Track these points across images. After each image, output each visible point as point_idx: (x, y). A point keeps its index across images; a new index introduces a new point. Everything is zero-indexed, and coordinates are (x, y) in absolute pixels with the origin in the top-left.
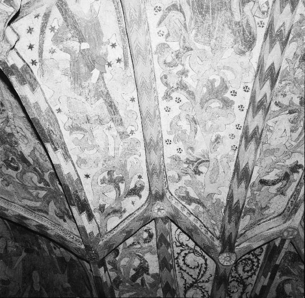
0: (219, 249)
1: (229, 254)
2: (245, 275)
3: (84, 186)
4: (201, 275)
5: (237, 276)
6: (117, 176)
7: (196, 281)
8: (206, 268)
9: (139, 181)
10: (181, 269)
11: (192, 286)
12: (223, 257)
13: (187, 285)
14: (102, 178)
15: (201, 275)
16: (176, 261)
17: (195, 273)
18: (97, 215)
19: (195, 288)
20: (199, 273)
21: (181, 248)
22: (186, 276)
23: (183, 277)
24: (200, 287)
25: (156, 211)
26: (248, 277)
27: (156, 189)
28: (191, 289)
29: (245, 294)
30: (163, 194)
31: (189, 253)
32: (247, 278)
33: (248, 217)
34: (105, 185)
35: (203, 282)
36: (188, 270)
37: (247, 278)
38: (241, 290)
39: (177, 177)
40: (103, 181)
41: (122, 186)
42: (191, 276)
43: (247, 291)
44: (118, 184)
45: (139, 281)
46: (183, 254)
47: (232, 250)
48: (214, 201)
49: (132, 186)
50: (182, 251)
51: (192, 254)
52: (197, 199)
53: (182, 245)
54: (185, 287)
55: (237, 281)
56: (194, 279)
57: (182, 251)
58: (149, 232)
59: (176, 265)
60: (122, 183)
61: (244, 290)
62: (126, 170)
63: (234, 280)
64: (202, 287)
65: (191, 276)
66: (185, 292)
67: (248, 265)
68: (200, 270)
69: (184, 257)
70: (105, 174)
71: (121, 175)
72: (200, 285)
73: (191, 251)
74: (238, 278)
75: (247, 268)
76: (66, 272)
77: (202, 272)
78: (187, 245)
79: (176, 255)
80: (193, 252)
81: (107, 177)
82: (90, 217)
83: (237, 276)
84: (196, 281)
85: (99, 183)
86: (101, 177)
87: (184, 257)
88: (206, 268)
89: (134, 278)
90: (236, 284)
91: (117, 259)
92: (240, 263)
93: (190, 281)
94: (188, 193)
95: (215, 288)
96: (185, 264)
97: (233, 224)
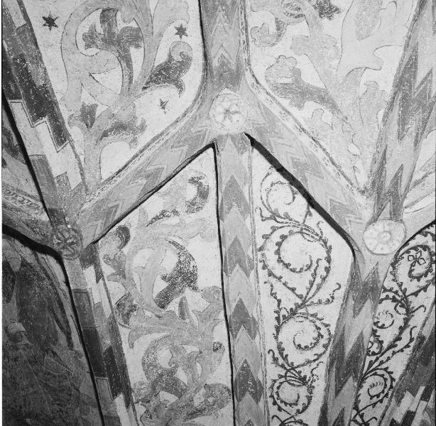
0: (367, 214)
1: (389, 225)
2: (412, 286)
3: (41, 48)
4: (315, 287)
5: (396, 288)
6: (125, 25)
7: (304, 302)
8: (327, 270)
9: (178, 43)
10: (270, 274)
11: (293, 313)
12: (375, 234)
13: (283, 312)
14: (86, 30)
15: (315, 287)
16: (259, 253)
17: (301, 282)
18: (75, 132)
19: (301, 319)
20: (312, 284)
21: (273, 223)
22: (279, 288)
23: (273, 295)
24: (312, 315)
25: (220, 118)
26: (419, 291)
27: (221, 51)
28: (291, 321)
29: (408, 330)
30: (239, 67)
31: (291, 233)
32: (416, 294)
34: (93, 51)
35: (320, 302)
37: (416, 294)
38: (399, 321)
39: (273, 29)
40: (90, 39)
41: (136, 54)
42: (293, 290)
43: (411, 323)
44: (126, 51)
45: (173, 306)
46: (276, 237)
48: (362, 89)
49: (161, 58)
50: (274, 229)
51: (299, 235)
52: (319, 90)
53: (274, 216)
54: (278, 319)
55: (394, 300)
56: (300, 297)
57: (274, 229)
58: (201, 184)
59: (260, 265)
60: (137, 46)
61: (406, 321)
62: (147, 9)
63: (387, 297)
64: (314, 315)
65: (293, 290)
66: (278, 329)
67: (422, 262)
68: (314, 275)
69: (279, 244)
70: (95, 17)
71: (134, 25)
72: (311, 310)
73: (296, 230)
74: (396, 292)
75: (419, 269)
76: (14, 298)
77: (318, 280)
78: (287, 216)
79: (260, 242)
80: (301, 232)
81: (100, 29)
82: (60, 135)
83: (396, 288)
84: (304, 302)
85: (81, 44)
86: (84, 28)
87: (279, 244)
88: (327, 270)
89: (163, 301)
91: (126, 250)
92: (406, 256)
93: (289, 302)
94: (297, 73)
95: (350, 312)
96: (280, 260)
97: (409, 140)
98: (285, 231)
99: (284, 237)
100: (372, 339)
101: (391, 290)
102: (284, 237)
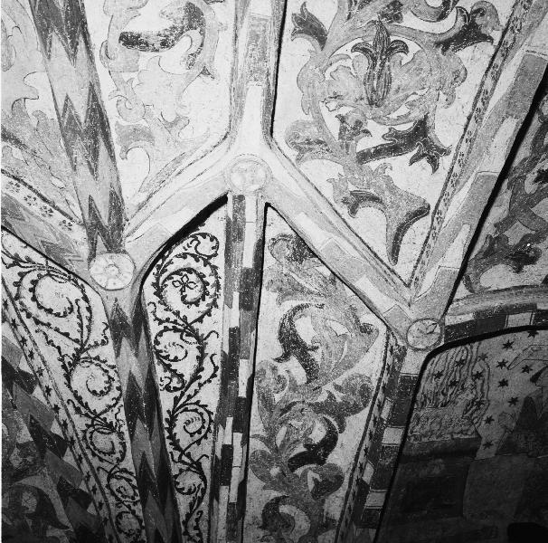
0: (84, 250)
1: (111, 257)
2: (192, 313)
4: (85, 329)
5: (173, 318)
7: (82, 345)
8: (89, 309)
10: (37, 322)
11: (76, 359)
12: (101, 270)
13: (67, 360)
15: (85, 329)
16: (17, 302)
17: (70, 325)
19: (86, 364)
20: (81, 325)
21: (17, 269)
22: (52, 334)
23: (50, 343)
24: (95, 359)
26: (203, 317)
28: (78, 367)
29: (207, 359)
31: (40, 276)
32: (200, 320)
33: (138, 154)
35: (96, 344)
36: (55, 322)
37: (200, 320)
38: (194, 352)
42: (67, 335)
43: (208, 350)
46: (27, 283)
47: (114, 246)
48: (34, 122)
50: (22, 275)
51: (48, 278)
54: (64, 367)
55: (175, 330)
56: (76, 341)
57: (22, 275)
59: (23, 315)
61: (201, 349)
63: (166, 329)
64: (97, 358)
65: (67, 335)
66: (68, 377)
67: (192, 285)
68: (79, 317)
72: (93, 353)
73: (44, 273)
74: (175, 322)
75: (192, 294)
77: (86, 322)
79: (14, 290)
80: (49, 275)
83: (173, 318)
84: (82, 345)
87: (32, 290)
88: (89, 309)
90: (175, 337)
92: (169, 282)
93: (69, 349)
97: (83, 170)
98: (34, 276)
99: (35, 283)
100: (168, 374)
101: (168, 320)
102: (35, 283)
